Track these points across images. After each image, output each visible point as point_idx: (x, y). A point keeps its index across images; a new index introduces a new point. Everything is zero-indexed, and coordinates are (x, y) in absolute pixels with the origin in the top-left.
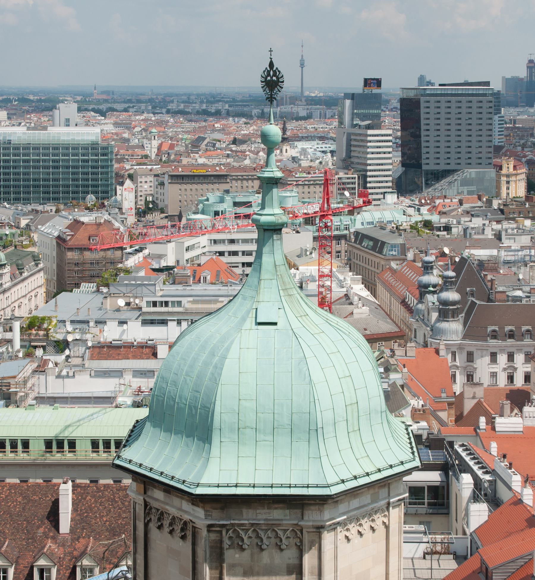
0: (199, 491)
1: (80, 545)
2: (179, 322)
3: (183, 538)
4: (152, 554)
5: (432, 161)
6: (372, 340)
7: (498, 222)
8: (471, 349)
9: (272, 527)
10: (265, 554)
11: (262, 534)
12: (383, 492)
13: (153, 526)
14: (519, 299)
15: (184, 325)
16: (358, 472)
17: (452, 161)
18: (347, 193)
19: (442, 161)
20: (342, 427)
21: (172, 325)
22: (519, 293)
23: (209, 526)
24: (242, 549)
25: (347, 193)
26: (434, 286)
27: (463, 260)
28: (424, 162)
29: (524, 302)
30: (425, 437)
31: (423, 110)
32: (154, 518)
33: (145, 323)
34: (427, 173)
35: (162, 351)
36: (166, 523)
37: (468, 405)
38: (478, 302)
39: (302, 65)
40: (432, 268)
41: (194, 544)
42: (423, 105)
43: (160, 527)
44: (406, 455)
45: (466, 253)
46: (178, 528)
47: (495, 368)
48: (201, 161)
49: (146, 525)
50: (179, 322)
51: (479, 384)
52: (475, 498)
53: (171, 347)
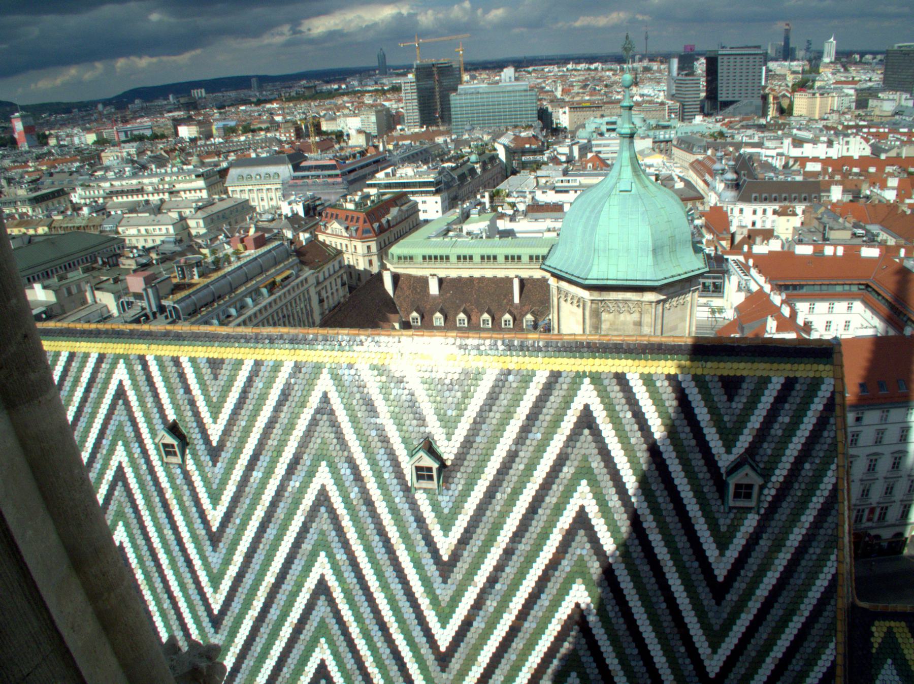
0: (587, 282)
1: (525, 309)
2: (576, 192)
3: (578, 306)
4: (562, 314)
5: (724, 95)
6: (684, 200)
7: (763, 132)
8: (742, 206)
9: (625, 301)
10: (622, 315)
11: (621, 305)
12: (688, 284)
13: (562, 300)
14: (770, 178)
15: (579, 192)
16: (674, 273)
17: (737, 95)
18: (673, 116)
19: (730, 96)
20: (666, 248)
21: (572, 192)
22: (772, 175)
23: (592, 300)
24: (610, 313)
25: (673, 116)
26: (723, 170)
27: (740, 155)
28: (719, 95)
29: (775, 179)
30: (713, 255)
31: (719, 64)
32: (563, 296)
33: (557, 192)
34: (721, 102)
35: (566, 208)
36: (569, 299)
37: (738, 238)
38: (748, 180)
39: (647, 38)
40: (721, 159)
41: (584, 309)
42: (719, 60)
43: (566, 301)
44: (702, 265)
45: (742, 151)
46: (575, 302)
47: (754, 218)
48: (587, 98)
49: (558, 299)
50: (576, 192)
51: (745, 227)
52: (740, 289)
53: (571, 204)
